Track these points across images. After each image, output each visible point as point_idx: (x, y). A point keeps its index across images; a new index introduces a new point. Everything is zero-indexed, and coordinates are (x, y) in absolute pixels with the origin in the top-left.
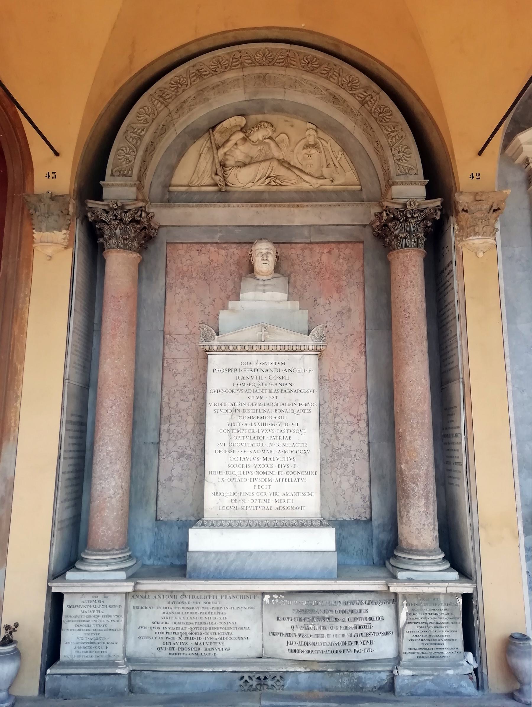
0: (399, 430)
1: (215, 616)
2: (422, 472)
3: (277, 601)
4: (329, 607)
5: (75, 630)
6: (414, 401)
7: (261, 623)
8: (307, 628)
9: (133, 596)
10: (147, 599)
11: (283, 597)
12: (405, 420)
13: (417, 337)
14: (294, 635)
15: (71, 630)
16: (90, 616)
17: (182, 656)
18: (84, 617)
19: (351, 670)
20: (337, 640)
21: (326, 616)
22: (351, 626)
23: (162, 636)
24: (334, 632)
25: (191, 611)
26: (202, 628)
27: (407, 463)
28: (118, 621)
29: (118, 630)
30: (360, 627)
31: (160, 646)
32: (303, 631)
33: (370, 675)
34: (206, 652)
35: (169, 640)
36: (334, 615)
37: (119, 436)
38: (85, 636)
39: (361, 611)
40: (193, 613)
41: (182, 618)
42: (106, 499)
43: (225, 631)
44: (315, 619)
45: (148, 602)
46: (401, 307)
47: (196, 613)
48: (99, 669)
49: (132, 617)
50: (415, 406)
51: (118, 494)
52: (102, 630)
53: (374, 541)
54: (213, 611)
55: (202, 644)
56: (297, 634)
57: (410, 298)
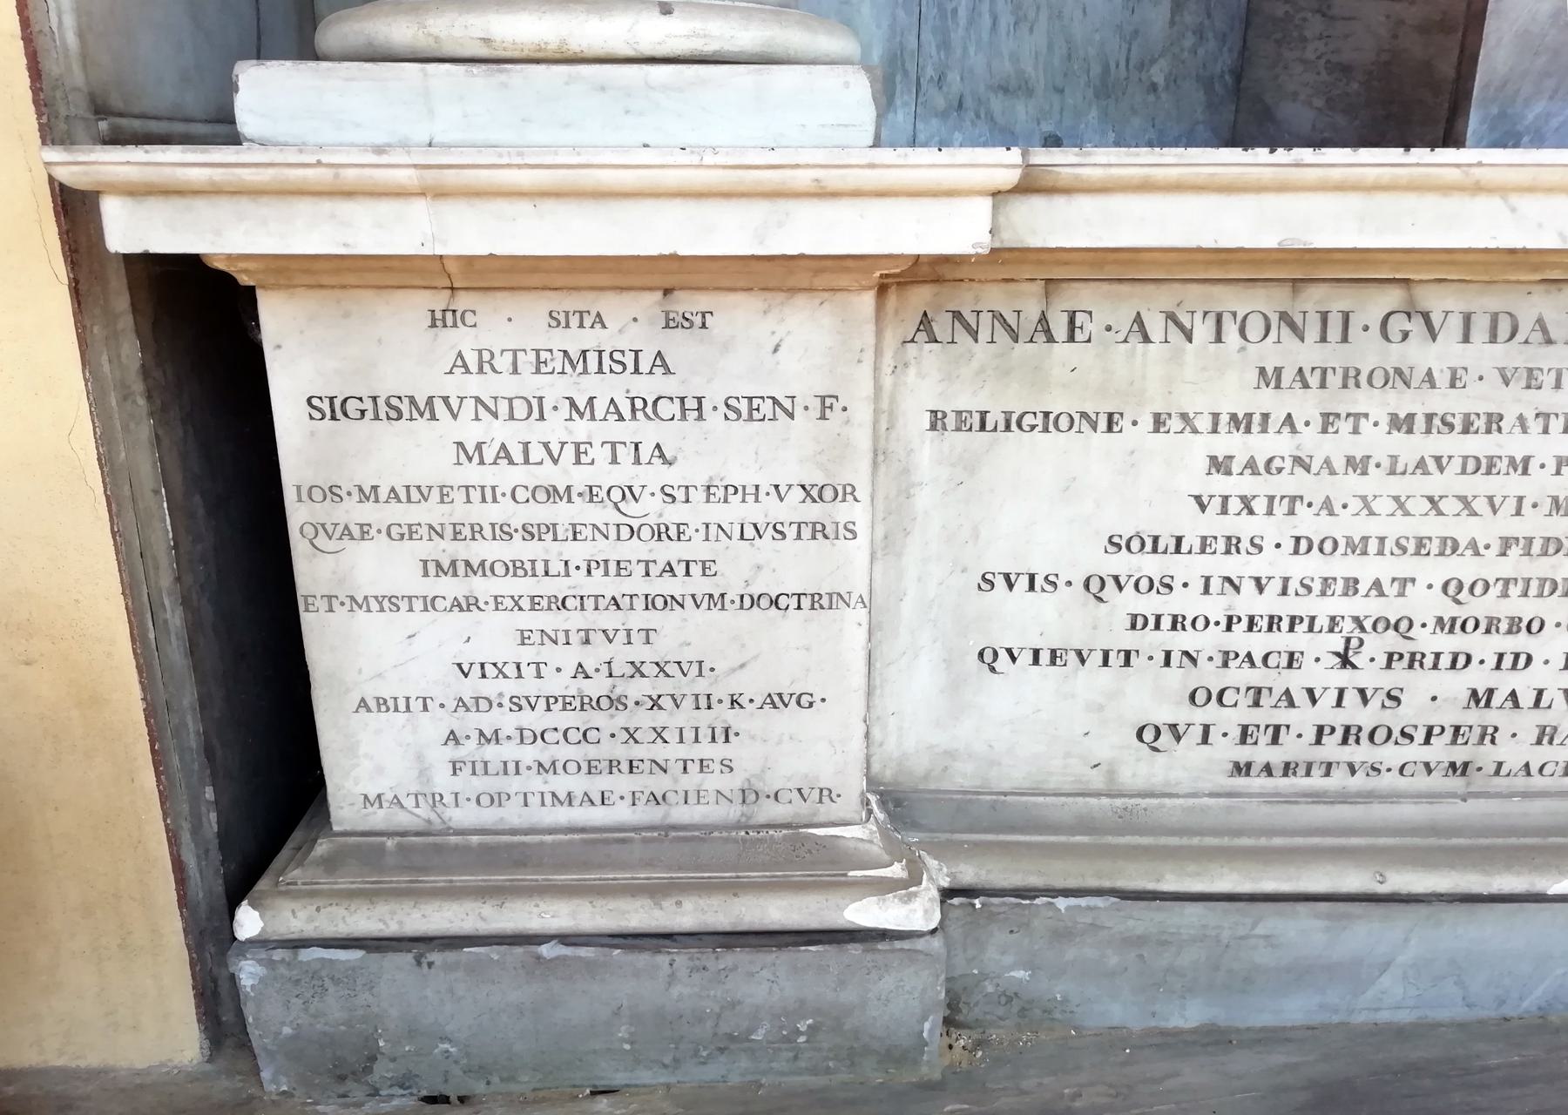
5: (430, 604)
9: (925, 322)
10: (1061, 350)
15: (390, 603)
16: (552, 493)
17: (1339, 779)
18: (489, 494)
25: (1478, 445)
28: (819, 530)
31: (1163, 716)
35: (1240, 676)
38: (527, 654)
40: (1489, 466)
41: (1384, 506)
45: (1067, 373)
47: (1523, 466)
48: (689, 904)
52: (671, 602)
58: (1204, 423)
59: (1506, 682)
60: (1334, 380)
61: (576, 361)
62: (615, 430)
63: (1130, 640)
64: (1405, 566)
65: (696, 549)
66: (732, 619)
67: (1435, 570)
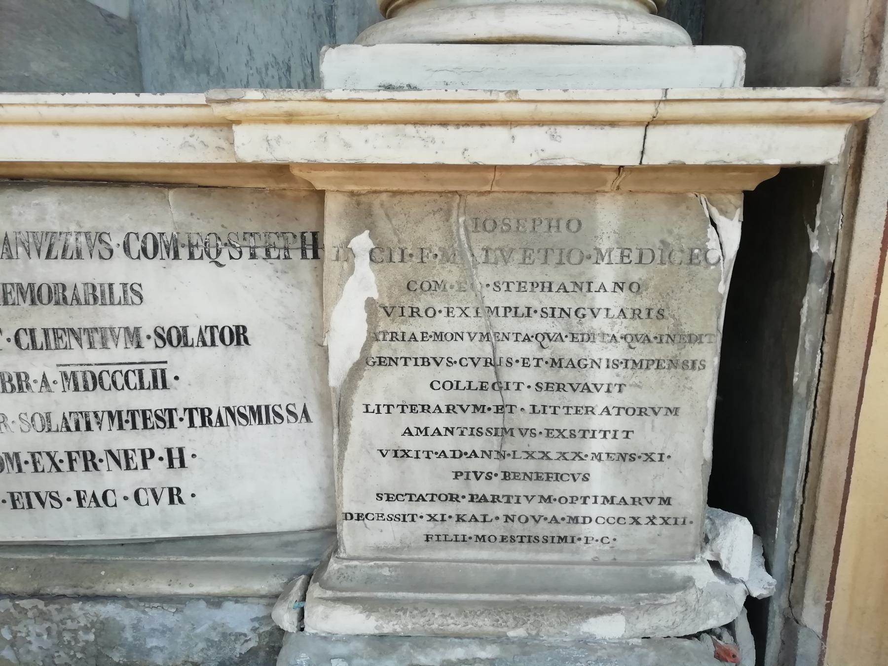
19: (57, 590)
33: (157, 617)
39: (99, 295)
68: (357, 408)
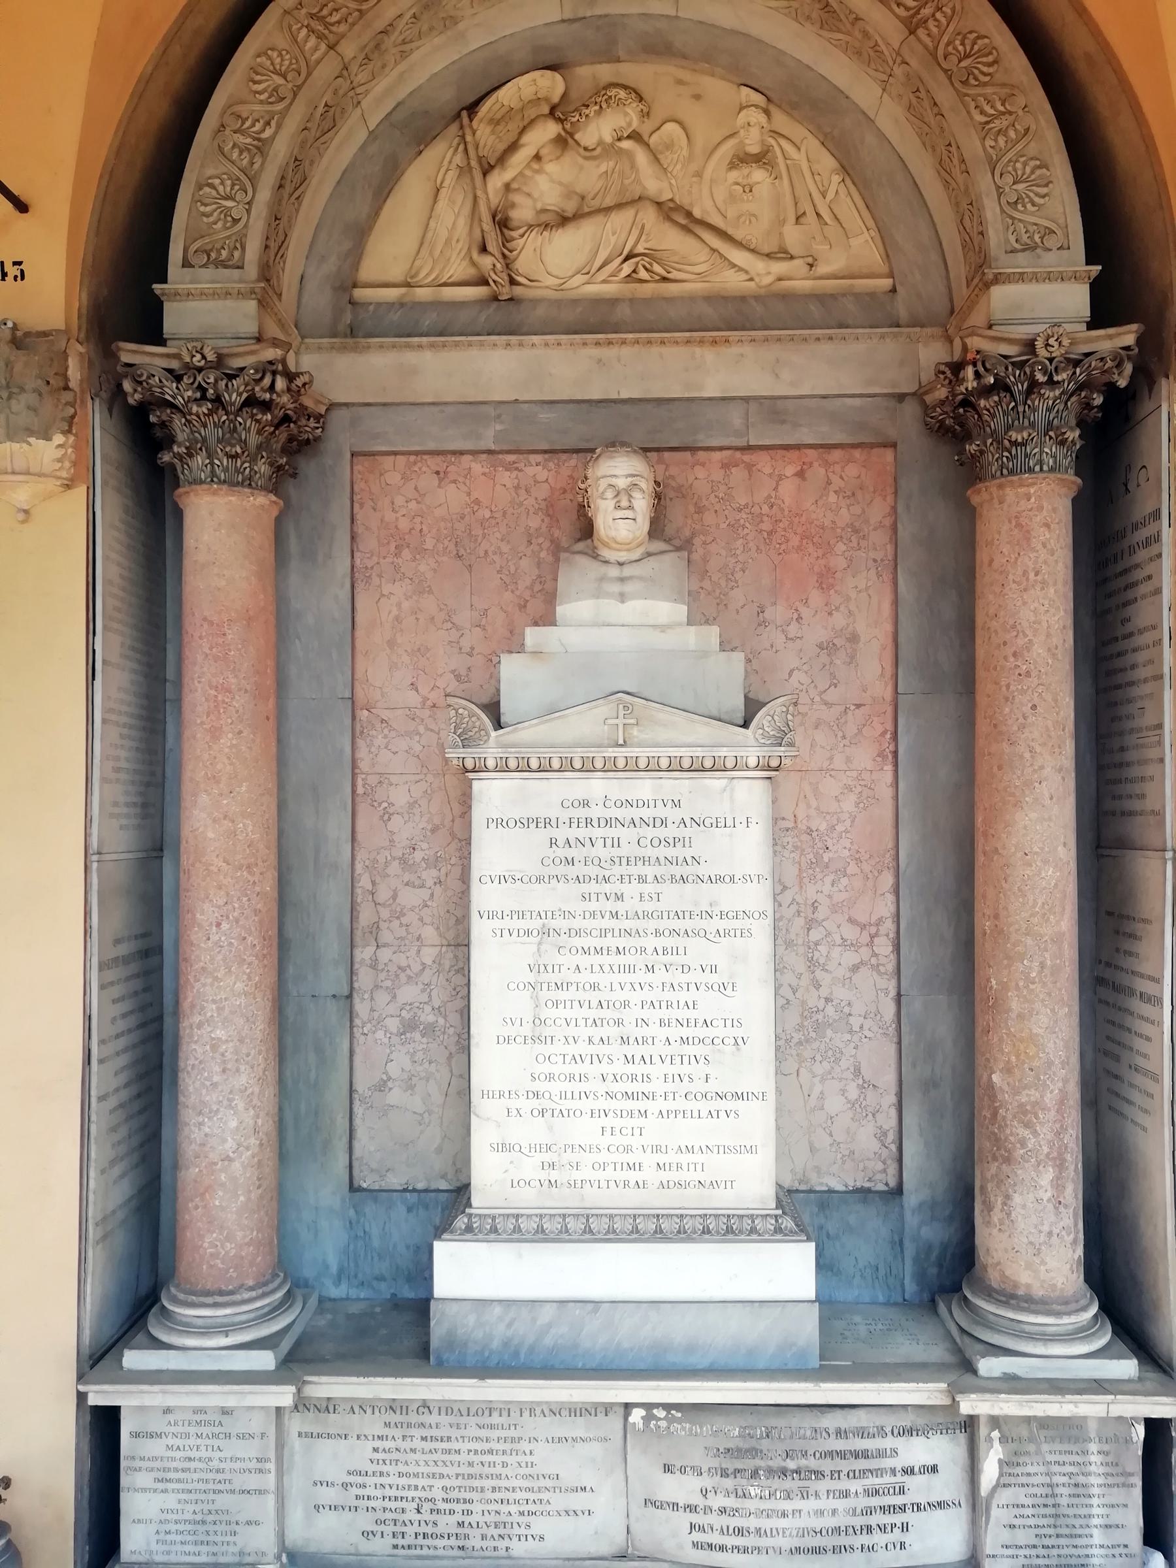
0: (988, 980)
1: (505, 1458)
2: (1050, 1099)
3: (663, 1424)
4: (798, 1445)
5: (155, 1491)
6: (1034, 906)
7: (622, 1477)
8: (740, 1493)
10: (332, 1415)
11: (679, 1415)
12: (1008, 957)
13: (1047, 729)
14: (708, 1510)
15: (144, 1490)
16: (190, 1459)
17: (425, 1552)
18: (173, 1459)
20: (818, 1523)
21: (791, 1465)
22: (853, 1491)
23: (372, 1504)
24: (812, 1504)
25: (445, 1445)
26: (472, 1489)
27: (1008, 1070)
28: (261, 1471)
29: (261, 1492)
30: (877, 1492)
31: (369, 1529)
32: (731, 1502)
34: (485, 1544)
36: (812, 1463)
37: (242, 1000)
38: (180, 1507)
39: (881, 1454)
40: (449, 1452)
41: (422, 1463)
42: (215, 1164)
43: (531, 1496)
44: (761, 1472)
46: (1005, 643)
47: (458, 1452)
49: (297, 1458)
50: (1035, 920)
51: (248, 1148)
52: (220, 1491)
53: (907, 1244)
54: (501, 1446)
55: (475, 1525)
56: (715, 1507)
57: (1033, 619)
58: (370, 1438)
59: (467, 1519)
60: (405, 1426)
61: (199, 1423)
62: (208, 1442)
63: (356, 1503)
64: (431, 1482)
65: (227, 1476)
66: (236, 1497)
67: (438, 1484)
68: (994, 1506)
